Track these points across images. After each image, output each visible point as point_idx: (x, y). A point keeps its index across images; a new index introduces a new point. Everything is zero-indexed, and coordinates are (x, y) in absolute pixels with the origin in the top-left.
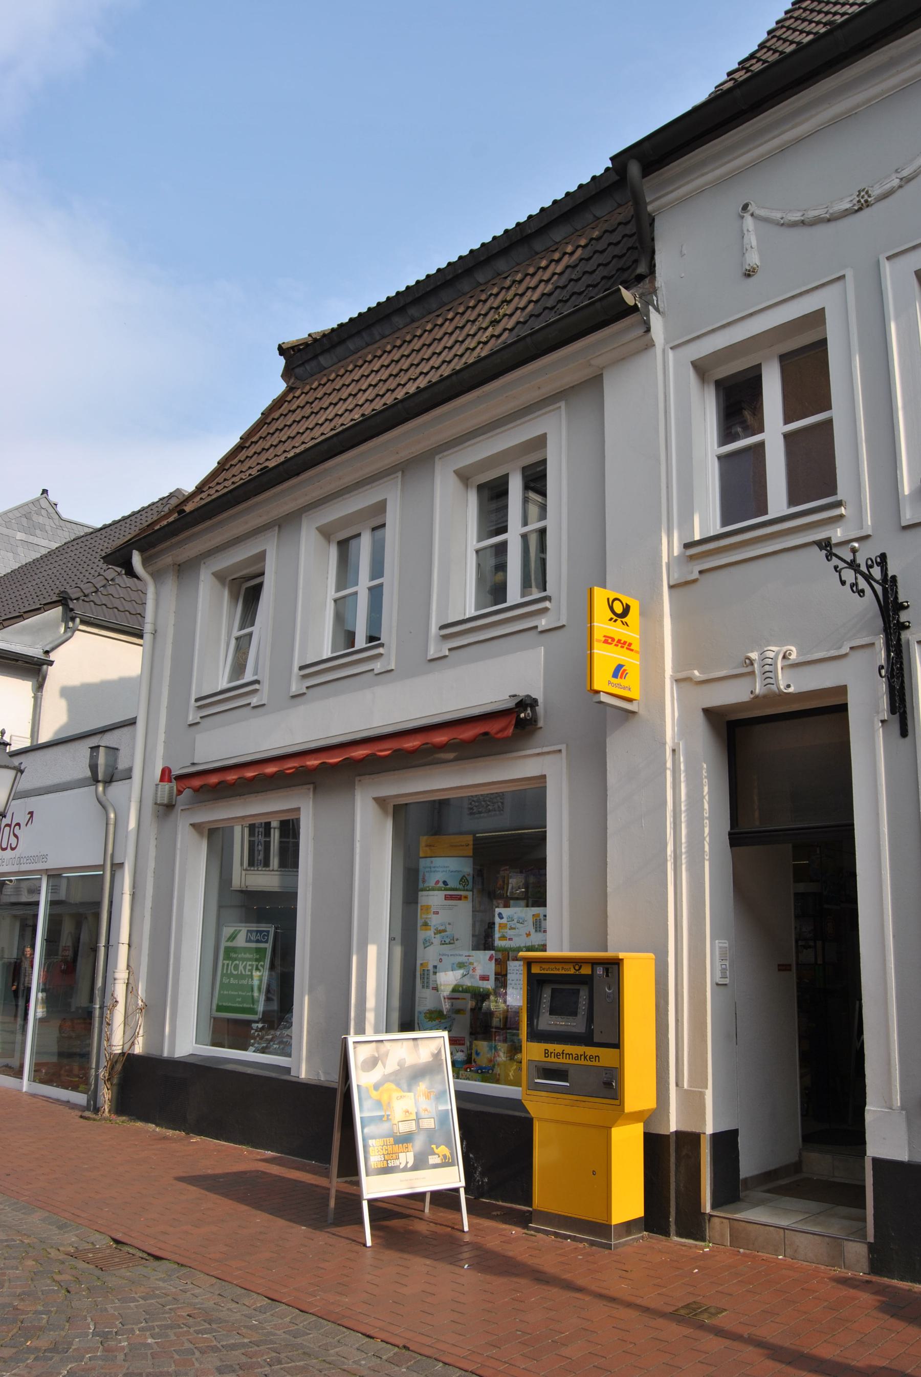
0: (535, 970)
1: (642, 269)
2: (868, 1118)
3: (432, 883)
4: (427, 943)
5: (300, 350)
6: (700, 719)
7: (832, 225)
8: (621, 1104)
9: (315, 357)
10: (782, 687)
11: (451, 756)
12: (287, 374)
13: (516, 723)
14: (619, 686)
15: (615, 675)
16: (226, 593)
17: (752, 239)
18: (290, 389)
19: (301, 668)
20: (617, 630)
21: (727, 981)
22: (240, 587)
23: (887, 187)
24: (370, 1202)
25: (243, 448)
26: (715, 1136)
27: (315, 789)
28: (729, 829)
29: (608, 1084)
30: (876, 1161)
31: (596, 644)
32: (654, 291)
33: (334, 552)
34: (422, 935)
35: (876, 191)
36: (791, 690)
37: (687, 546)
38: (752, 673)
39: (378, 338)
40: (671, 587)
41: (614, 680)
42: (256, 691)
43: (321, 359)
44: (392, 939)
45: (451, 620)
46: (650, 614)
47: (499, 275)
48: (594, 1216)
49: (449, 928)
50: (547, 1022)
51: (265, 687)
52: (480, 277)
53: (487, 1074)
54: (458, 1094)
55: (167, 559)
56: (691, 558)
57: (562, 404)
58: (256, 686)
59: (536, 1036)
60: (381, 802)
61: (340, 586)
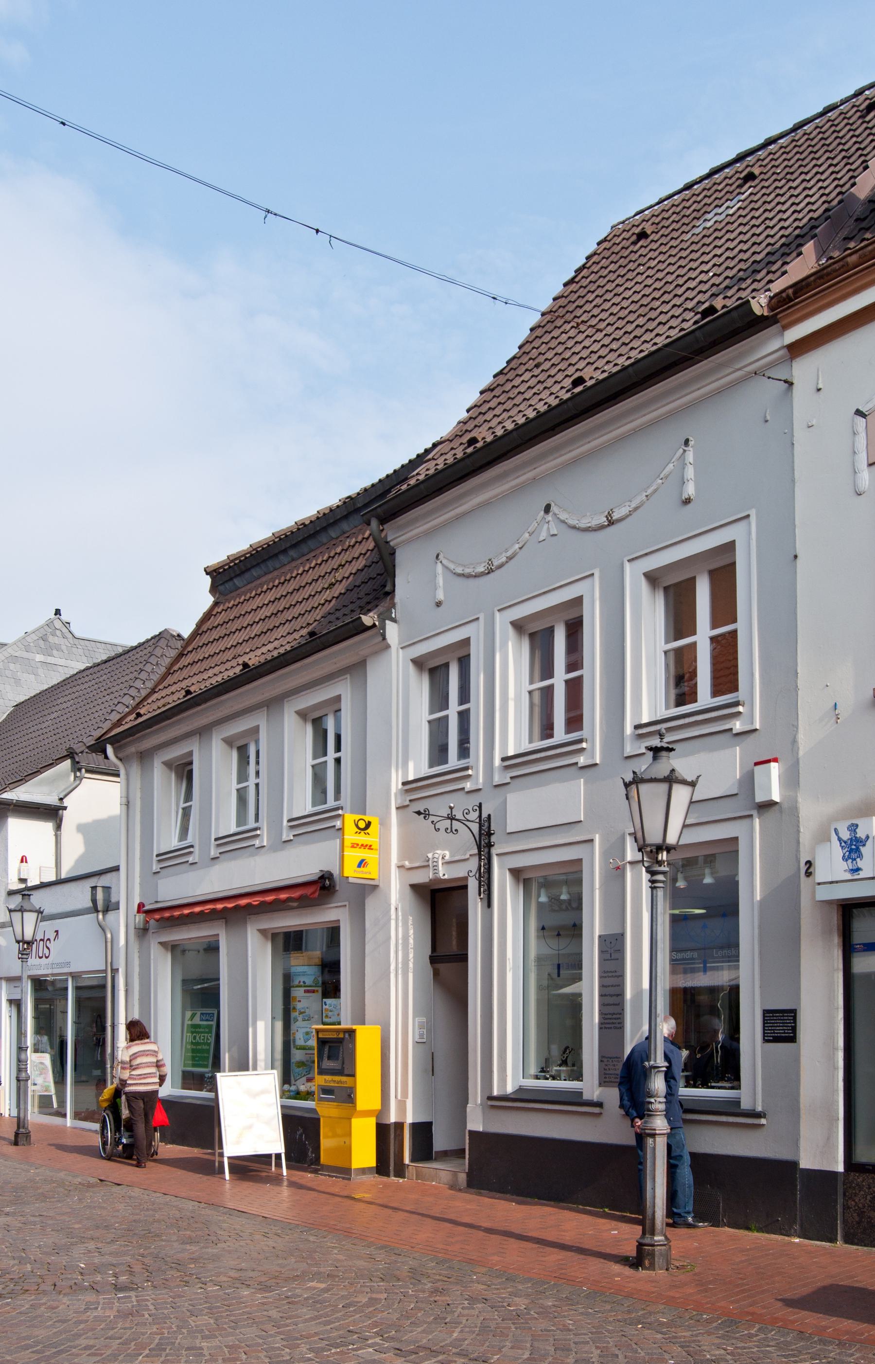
0: (321, 1036)
1: (388, 588)
2: (468, 1110)
3: (296, 983)
4: (296, 1020)
5: (220, 573)
6: (408, 890)
7: (477, 580)
8: (355, 1106)
9: (231, 579)
10: (441, 875)
11: (295, 904)
12: (213, 590)
13: (323, 887)
14: (362, 872)
15: (359, 866)
16: (173, 775)
17: (440, 581)
18: (216, 604)
19: (216, 840)
20: (362, 838)
21: (424, 1040)
22: (184, 770)
23: (500, 561)
24: (229, 1158)
25: (183, 655)
26: (415, 1126)
27: (226, 922)
28: (429, 953)
29: (350, 1096)
30: (470, 1132)
31: (346, 849)
32: (394, 605)
33: (235, 754)
34: (294, 1014)
35: (496, 563)
36: (446, 877)
37: (404, 784)
38: (429, 866)
39: (272, 569)
40: (397, 808)
41: (359, 869)
42: (191, 853)
43: (235, 581)
44: (273, 1018)
45: (295, 816)
46: (384, 823)
47: (344, 533)
48: (345, 1166)
49: (307, 1011)
50: (327, 1064)
51: (196, 850)
52: (333, 533)
53: (298, 1095)
54: (282, 1107)
55: (132, 749)
56: (407, 791)
57: (348, 676)
58: (192, 850)
59: (321, 1072)
60: (263, 932)
61: (240, 781)
